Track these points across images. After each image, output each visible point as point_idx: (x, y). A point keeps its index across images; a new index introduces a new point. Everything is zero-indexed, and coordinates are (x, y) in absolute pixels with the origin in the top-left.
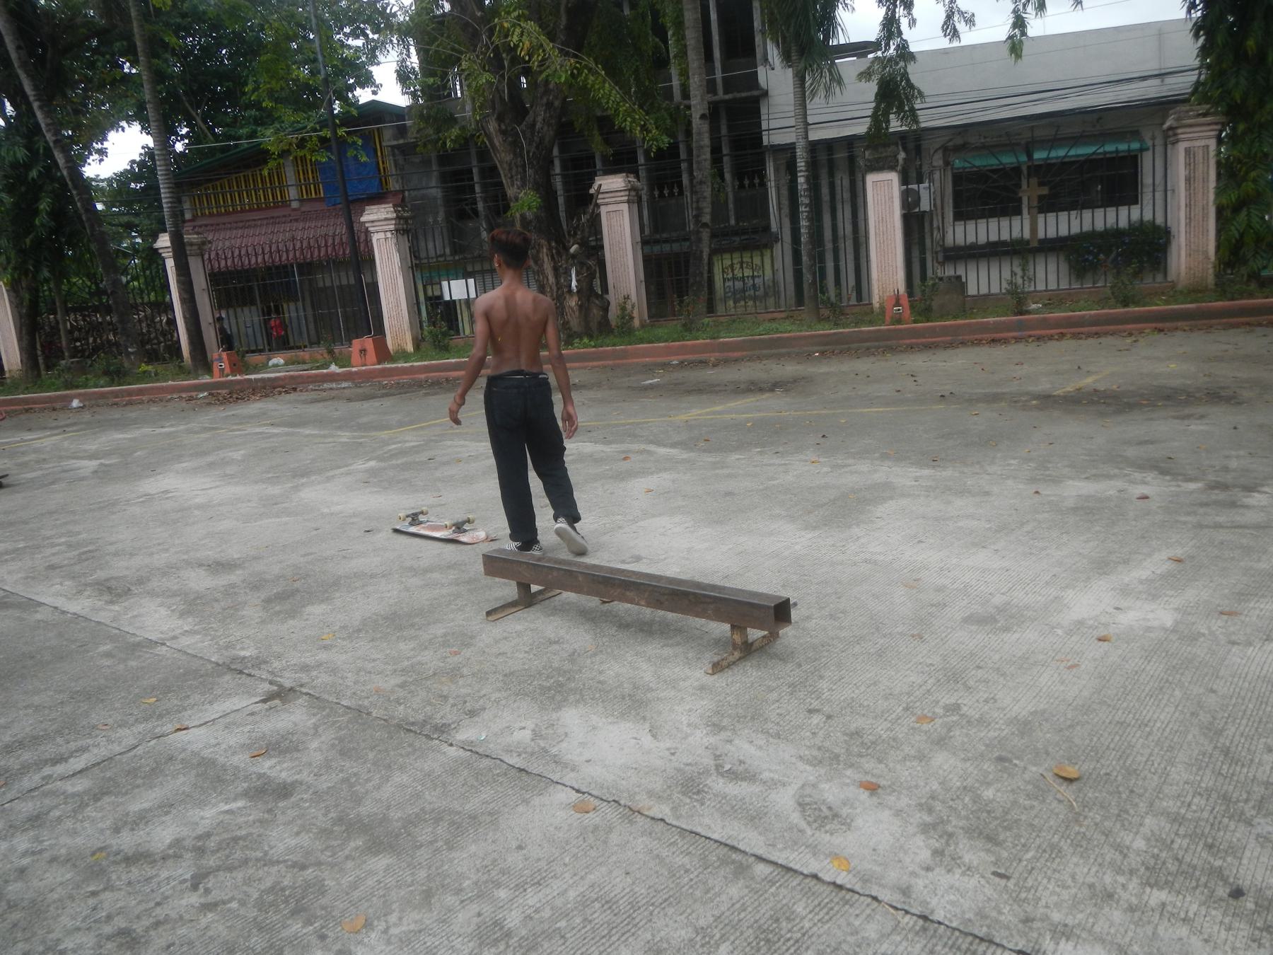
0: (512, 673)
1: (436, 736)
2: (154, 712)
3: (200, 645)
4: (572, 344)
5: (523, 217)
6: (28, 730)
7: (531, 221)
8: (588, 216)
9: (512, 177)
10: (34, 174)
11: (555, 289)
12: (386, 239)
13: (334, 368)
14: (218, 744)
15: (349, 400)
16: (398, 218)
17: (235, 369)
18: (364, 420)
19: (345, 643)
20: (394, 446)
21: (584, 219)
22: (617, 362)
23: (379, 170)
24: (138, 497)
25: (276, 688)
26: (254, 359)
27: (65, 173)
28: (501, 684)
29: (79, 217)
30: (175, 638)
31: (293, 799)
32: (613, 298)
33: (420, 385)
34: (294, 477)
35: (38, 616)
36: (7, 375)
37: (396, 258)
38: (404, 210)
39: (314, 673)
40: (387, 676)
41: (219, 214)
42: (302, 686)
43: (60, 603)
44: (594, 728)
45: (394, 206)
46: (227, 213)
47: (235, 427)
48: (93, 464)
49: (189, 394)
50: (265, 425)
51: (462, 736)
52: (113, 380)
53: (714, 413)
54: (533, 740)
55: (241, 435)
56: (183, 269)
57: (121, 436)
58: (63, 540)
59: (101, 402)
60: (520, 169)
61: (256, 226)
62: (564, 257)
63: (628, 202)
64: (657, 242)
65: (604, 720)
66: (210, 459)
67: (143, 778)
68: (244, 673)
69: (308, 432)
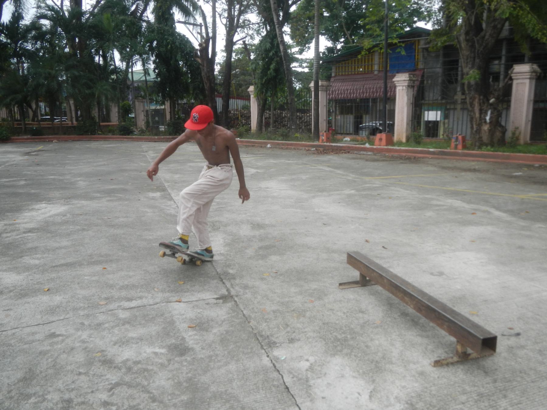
0: (328, 323)
1: (265, 348)
5: (469, 83)
7: (472, 85)
9: (467, 63)
10: (271, 54)
11: (478, 120)
12: (403, 89)
13: (367, 145)
15: (367, 160)
16: (410, 80)
17: (328, 140)
18: (366, 170)
23: (415, 58)
26: (339, 137)
27: (282, 54)
28: (317, 328)
29: (284, 72)
31: (183, 358)
32: (510, 128)
33: (401, 158)
37: (406, 99)
40: (273, 304)
41: (345, 75)
44: (343, 376)
45: (409, 75)
46: (348, 75)
47: (314, 165)
50: (325, 166)
51: (276, 353)
52: (284, 138)
53: (543, 197)
54: (307, 370)
59: (277, 146)
62: (486, 105)
63: (530, 79)
65: (351, 373)
66: (294, 177)
69: (338, 171)
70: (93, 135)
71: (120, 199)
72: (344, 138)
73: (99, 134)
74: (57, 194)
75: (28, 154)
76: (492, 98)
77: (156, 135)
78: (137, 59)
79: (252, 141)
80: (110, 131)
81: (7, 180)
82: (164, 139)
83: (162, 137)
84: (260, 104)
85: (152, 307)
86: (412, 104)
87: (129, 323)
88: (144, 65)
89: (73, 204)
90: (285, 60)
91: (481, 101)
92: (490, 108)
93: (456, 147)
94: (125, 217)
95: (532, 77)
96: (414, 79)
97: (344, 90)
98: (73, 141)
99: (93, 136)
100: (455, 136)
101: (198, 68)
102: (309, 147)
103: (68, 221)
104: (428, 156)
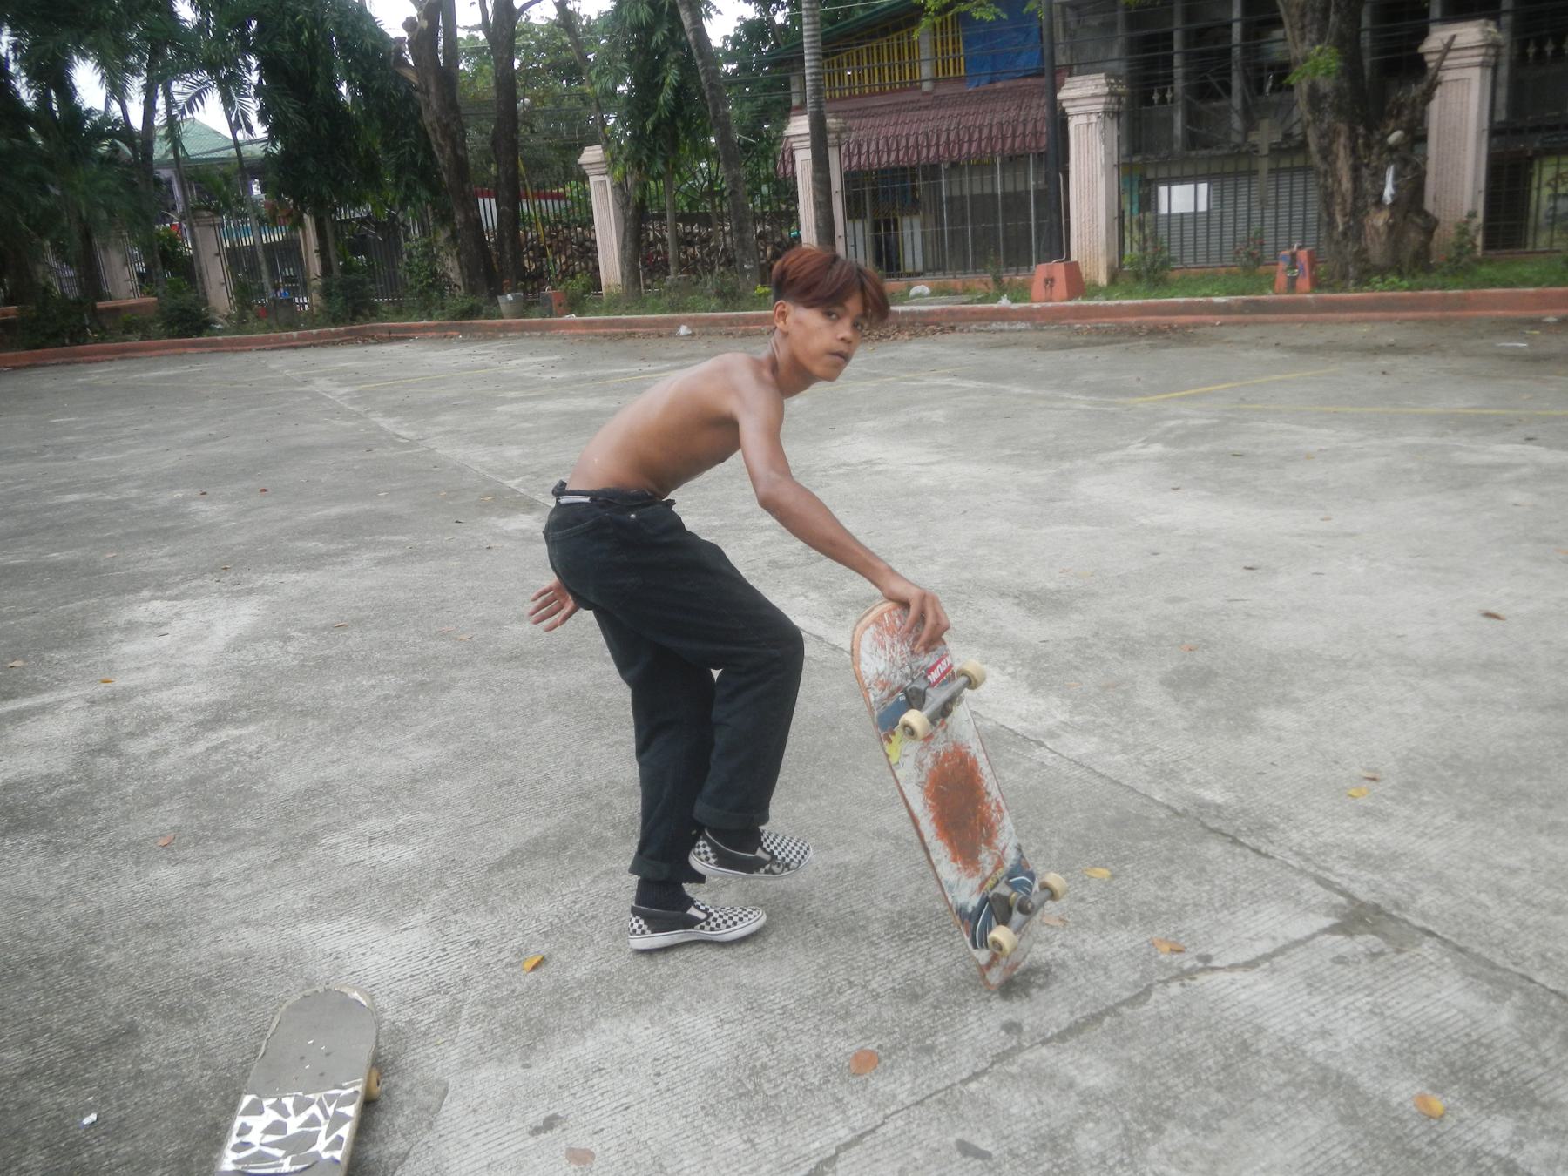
3: (1109, 759)
4: (1368, 283)
5: (1313, 88)
6: (910, 890)
7: (1325, 96)
8: (1424, 86)
9: (1303, 27)
10: (658, 37)
11: (1349, 200)
12: (1089, 124)
13: (1004, 302)
14: (1324, 1034)
15: (1042, 347)
16: (1111, 94)
18: (1092, 377)
19: (1405, 811)
20: (1172, 423)
21: (1416, 90)
22: (1449, 313)
24: (839, 466)
25: (1342, 900)
27: (690, 37)
29: (702, 97)
30: (1051, 735)
33: (1134, 333)
34: (1048, 457)
36: (604, 291)
37: (1099, 153)
38: (1118, 84)
39: (1400, 877)
42: (1397, 905)
45: (1107, 77)
46: (842, 98)
52: (726, 304)
59: (712, 329)
60: (1318, 15)
62: (1376, 150)
63: (1482, 65)
64: (1517, 131)
67: (1220, 1090)
68: (1242, 845)
69: (1017, 390)
70: (79, 344)
71: (414, 554)
72: (911, 287)
73: (96, 342)
74: (160, 557)
76: (1392, 132)
77: (292, 326)
80: (129, 328)
82: (319, 336)
83: (315, 331)
84: (628, 203)
85: (1148, 1008)
86: (1118, 166)
87: (1170, 1115)
88: (227, 102)
89: (263, 590)
90: (701, 56)
91: (1360, 141)
92: (1393, 161)
93: (1292, 285)
95: (1487, 59)
96: (1120, 90)
98: (15, 368)
99: (80, 347)
100: (1287, 252)
101: (409, 98)
103: (325, 658)
104: (1209, 318)
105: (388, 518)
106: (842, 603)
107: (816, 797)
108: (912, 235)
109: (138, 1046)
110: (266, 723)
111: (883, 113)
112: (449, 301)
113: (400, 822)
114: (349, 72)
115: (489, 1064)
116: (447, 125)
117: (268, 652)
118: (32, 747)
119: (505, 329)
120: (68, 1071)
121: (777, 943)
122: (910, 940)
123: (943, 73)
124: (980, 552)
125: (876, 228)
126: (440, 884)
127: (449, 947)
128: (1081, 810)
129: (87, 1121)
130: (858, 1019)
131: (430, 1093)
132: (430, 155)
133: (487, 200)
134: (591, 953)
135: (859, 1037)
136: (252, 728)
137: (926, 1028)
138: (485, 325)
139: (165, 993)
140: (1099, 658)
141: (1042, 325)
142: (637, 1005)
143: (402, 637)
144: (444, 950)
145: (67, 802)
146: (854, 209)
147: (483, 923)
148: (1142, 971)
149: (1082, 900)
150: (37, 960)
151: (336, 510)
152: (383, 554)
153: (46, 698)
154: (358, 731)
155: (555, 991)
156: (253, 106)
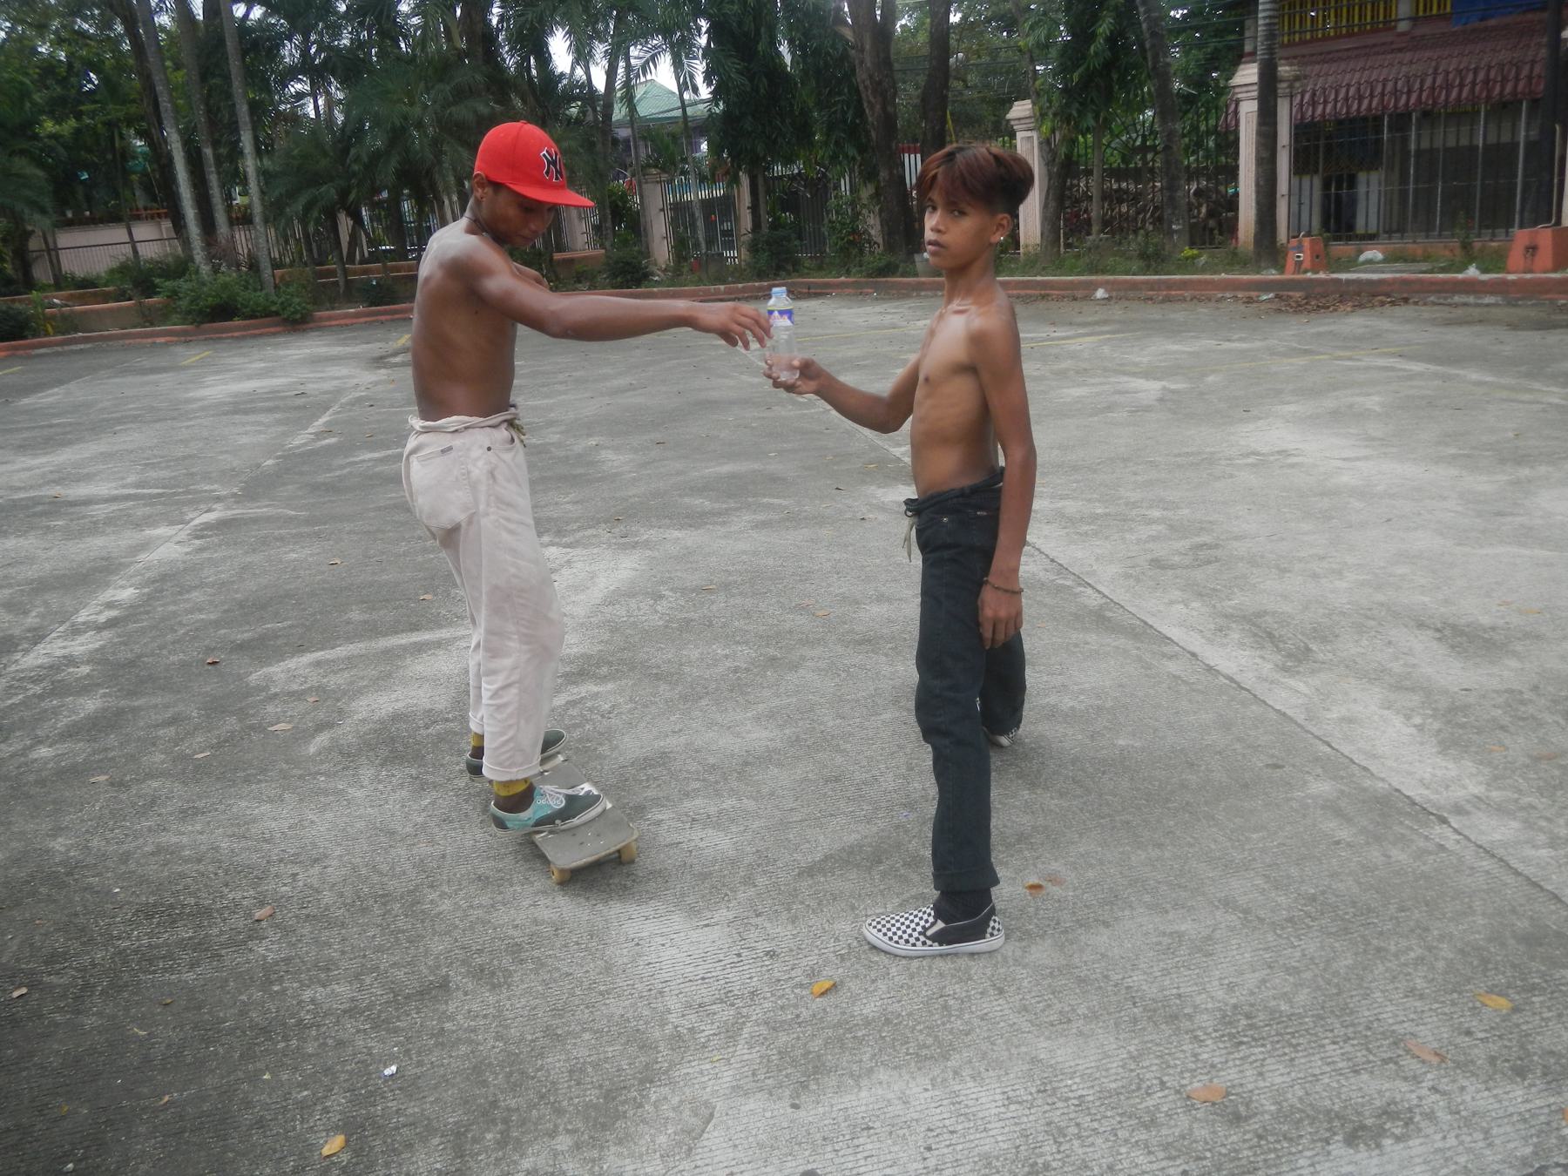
2: (1529, 1055)
3: (1531, 852)
6: (1251, 980)
13: (1472, 272)
15: (1514, 326)
17: (1322, 260)
24: (1248, 455)
26: (1341, 249)
30: (1459, 810)
34: (1503, 461)
35: (1173, 667)
36: (1021, 250)
43: (1195, 643)
46: (1303, 42)
47: (1341, 353)
48: (1150, 389)
49: (1247, 294)
50: (1393, 355)
52: (1148, 267)
55: (1358, 369)
56: (1267, 116)
57: (1176, 347)
58: (1156, 513)
59: (1131, 294)
61: (1340, 59)
66: (1329, 403)
69: (1474, 375)
71: (792, 520)
72: (1361, 252)
75: (379, 361)
78: (655, 47)
79: (1038, 283)
81: (376, 455)
82: (744, 290)
88: (677, 65)
89: (647, 544)
94: (881, 598)
97: (1324, 89)
101: (844, 57)
102: (1249, 290)
103: (688, 621)
105: (774, 479)
106: (1226, 616)
107: (1160, 846)
108: (1371, 191)
109: (446, 1003)
110: (623, 682)
111: (1349, 57)
112: (867, 258)
113: (724, 806)
114: (790, 30)
115: (759, 1095)
116: (880, 83)
117: (639, 609)
118: (422, 679)
119: (919, 287)
120: (383, 1016)
121: (1086, 1017)
122: (1242, 1043)
123: (1425, 10)
124: (1401, 570)
125: (1326, 185)
126: (748, 881)
127: (745, 953)
128: (1484, 914)
129: (388, 1072)
130: (1164, 1132)
131: (696, 1115)
132: (860, 113)
133: (912, 156)
134: (884, 988)
135: (1161, 1155)
136: (610, 686)
137: (1244, 1162)
138: (900, 283)
139: (480, 951)
140: (1533, 717)
141: (1519, 299)
142: (921, 1059)
143: (762, 606)
144: (739, 955)
145: (440, 738)
146: (1301, 165)
147: (782, 932)
148: (1535, 1145)
149: (1468, 1033)
150: (383, 896)
151: (727, 468)
152: (761, 517)
153: (444, 634)
154: (704, 702)
155: (839, 1025)
156: (699, 67)
